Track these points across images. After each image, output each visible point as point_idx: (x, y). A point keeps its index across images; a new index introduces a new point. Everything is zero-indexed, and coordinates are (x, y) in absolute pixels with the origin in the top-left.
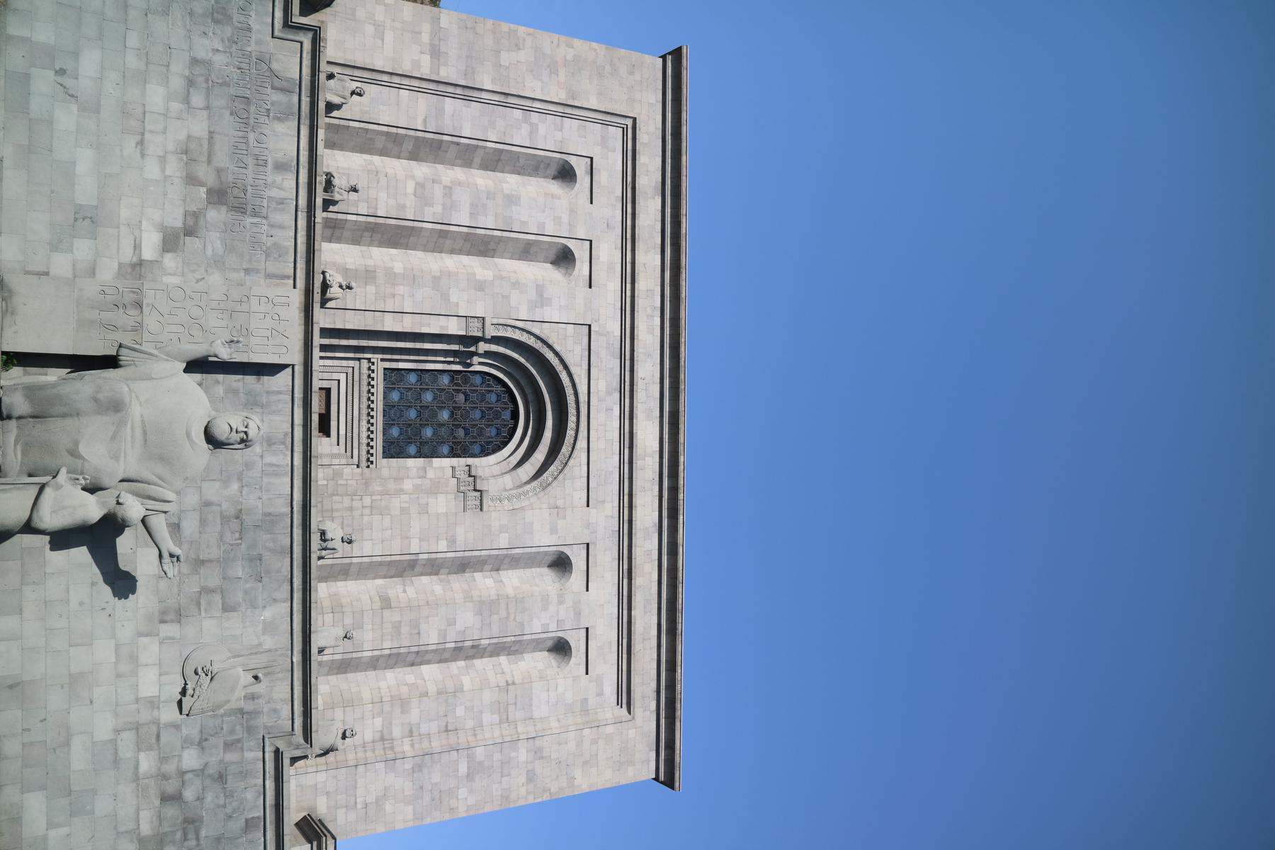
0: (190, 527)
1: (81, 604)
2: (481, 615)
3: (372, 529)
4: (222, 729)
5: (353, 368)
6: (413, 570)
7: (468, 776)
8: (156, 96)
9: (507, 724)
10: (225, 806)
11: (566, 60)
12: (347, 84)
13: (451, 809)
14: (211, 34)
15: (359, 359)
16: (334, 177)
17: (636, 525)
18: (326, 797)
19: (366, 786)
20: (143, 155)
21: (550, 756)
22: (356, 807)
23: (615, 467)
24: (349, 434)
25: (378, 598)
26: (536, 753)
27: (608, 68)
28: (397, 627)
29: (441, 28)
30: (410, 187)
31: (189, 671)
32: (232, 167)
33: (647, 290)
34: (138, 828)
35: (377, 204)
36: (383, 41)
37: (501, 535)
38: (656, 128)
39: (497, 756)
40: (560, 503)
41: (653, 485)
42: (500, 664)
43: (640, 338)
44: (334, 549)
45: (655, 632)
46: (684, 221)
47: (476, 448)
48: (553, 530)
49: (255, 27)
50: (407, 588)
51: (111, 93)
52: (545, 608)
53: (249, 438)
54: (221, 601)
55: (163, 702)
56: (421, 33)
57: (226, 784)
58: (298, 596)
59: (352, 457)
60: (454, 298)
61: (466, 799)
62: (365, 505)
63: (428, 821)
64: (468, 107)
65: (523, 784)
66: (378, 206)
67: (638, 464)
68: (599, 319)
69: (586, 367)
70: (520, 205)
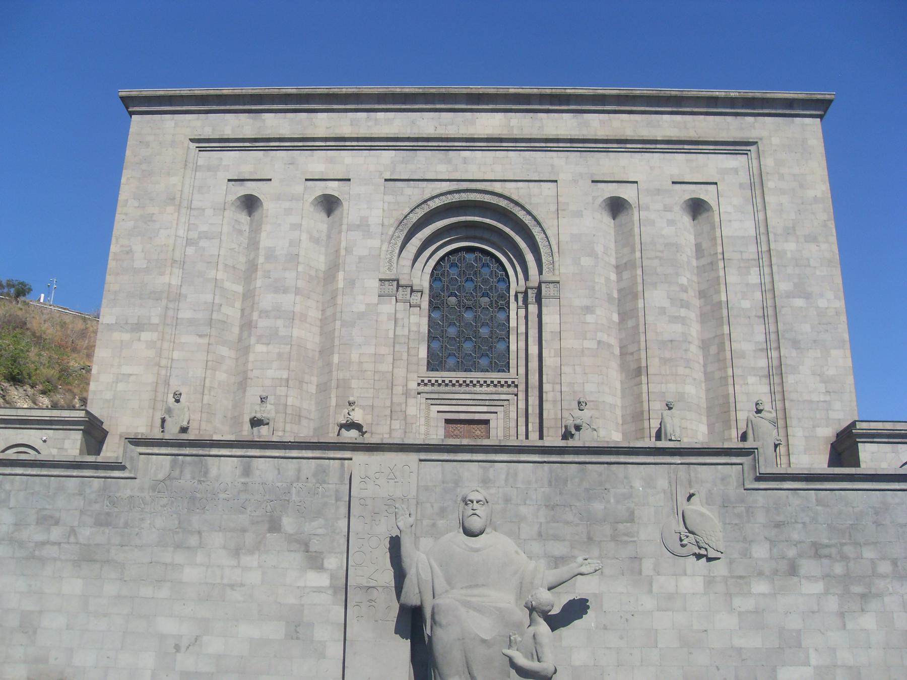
0: (559, 549)
1: (621, 638)
2: (656, 283)
3: (574, 383)
4: (736, 524)
5: (426, 399)
6: (613, 346)
8: (191, 574)
9: (761, 260)
10: (804, 523)
11: (139, 207)
12: (171, 406)
13: (837, 315)
14: (137, 530)
16: (255, 417)
17: (575, 135)
18: (817, 429)
20: (242, 585)
21: (793, 220)
23: (520, 155)
24: (487, 403)
26: (788, 234)
27: (144, 167)
28: (664, 361)
29: (116, 323)
30: (260, 348)
31: (684, 551)
32: (248, 511)
33: (352, 125)
34: (817, 594)
35: (278, 379)
36: (131, 375)
37: (582, 264)
38: (198, 119)
39: (790, 270)
40: (553, 208)
41: (537, 119)
42: (703, 266)
43: (397, 132)
44: (591, 417)
46: (284, 90)
47: (502, 286)
48: (579, 214)
49: (128, 493)
50: (630, 351)
51: (192, 610)
52: (652, 223)
53: (483, 499)
54: (625, 524)
55: (709, 573)
56: (122, 341)
57: (784, 522)
58: (622, 459)
59: (508, 400)
60: (362, 308)
61: (828, 300)
62: (552, 390)
63: (846, 336)
64: (186, 297)
65: (817, 246)
66: (279, 377)
67: (516, 134)
68: (380, 172)
69: (425, 184)
70: (275, 247)
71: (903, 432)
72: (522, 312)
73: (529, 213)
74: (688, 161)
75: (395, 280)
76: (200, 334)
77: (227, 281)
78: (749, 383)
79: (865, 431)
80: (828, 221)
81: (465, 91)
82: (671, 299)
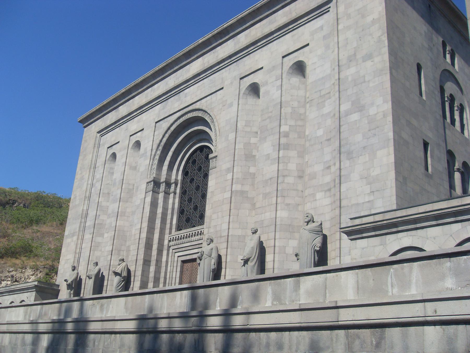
2: (266, 137)
3: (216, 226)
6: (248, 191)
7: (360, 111)
11: (81, 174)
13: (384, 117)
15: (169, 247)
19: (358, 196)
21: (355, 48)
22: (372, 201)
24: (197, 246)
36: (69, 259)
48: (231, 105)
61: (378, 106)
62: (207, 233)
65: (372, 61)
66: (109, 250)
71: (385, 222)
74: (293, 36)
75: (151, 181)
77: (104, 201)
78: (317, 199)
79: (350, 229)
80: (381, 36)
81: (181, 54)
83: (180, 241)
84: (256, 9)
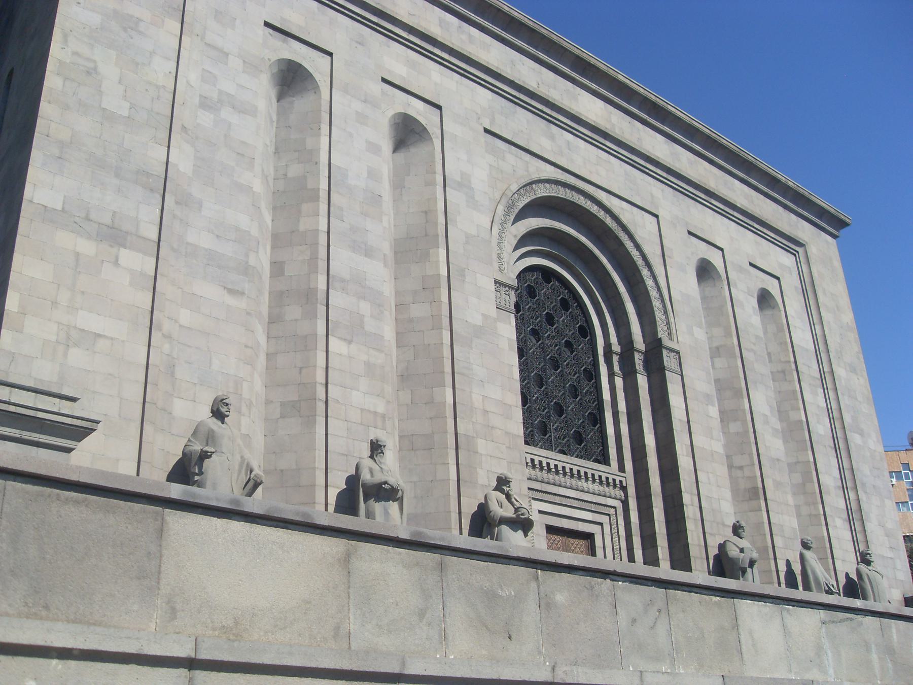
12: (215, 428)
16: (385, 483)
24: (593, 507)
25: (754, 503)
29: (63, 210)
33: (440, 26)
35: (369, 411)
36: (99, 336)
45: (745, 188)
56: (77, 255)
60: (478, 320)
62: (690, 503)
64: (200, 205)
66: (372, 409)
69: (527, 157)
72: (619, 382)
73: (638, 247)
76: (230, 287)
81: (577, 52)
82: (770, 406)
83: (551, 477)
84: (719, 143)
